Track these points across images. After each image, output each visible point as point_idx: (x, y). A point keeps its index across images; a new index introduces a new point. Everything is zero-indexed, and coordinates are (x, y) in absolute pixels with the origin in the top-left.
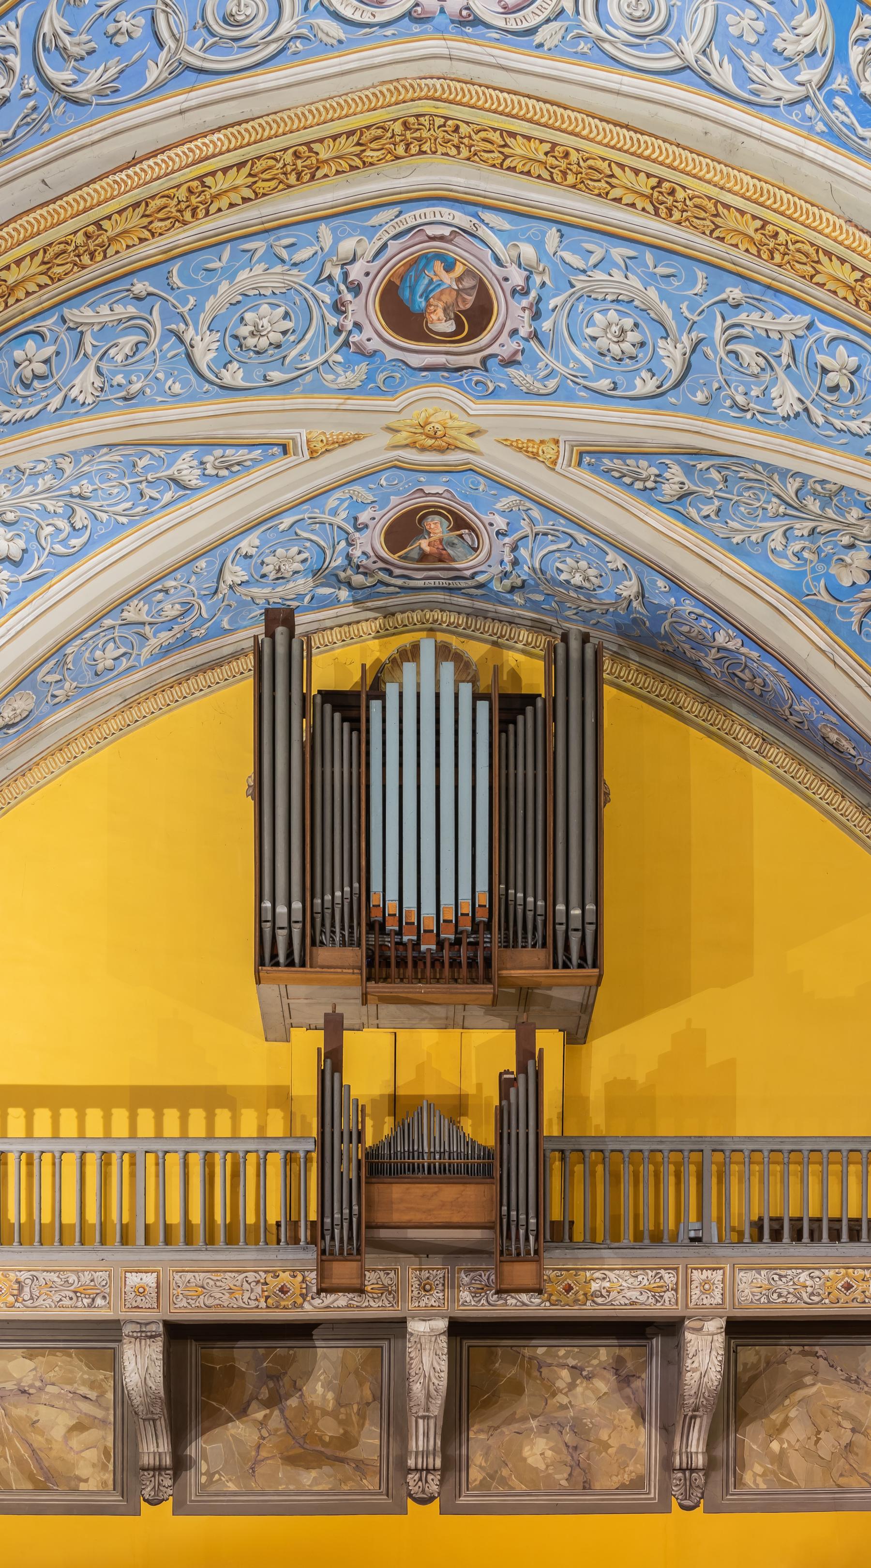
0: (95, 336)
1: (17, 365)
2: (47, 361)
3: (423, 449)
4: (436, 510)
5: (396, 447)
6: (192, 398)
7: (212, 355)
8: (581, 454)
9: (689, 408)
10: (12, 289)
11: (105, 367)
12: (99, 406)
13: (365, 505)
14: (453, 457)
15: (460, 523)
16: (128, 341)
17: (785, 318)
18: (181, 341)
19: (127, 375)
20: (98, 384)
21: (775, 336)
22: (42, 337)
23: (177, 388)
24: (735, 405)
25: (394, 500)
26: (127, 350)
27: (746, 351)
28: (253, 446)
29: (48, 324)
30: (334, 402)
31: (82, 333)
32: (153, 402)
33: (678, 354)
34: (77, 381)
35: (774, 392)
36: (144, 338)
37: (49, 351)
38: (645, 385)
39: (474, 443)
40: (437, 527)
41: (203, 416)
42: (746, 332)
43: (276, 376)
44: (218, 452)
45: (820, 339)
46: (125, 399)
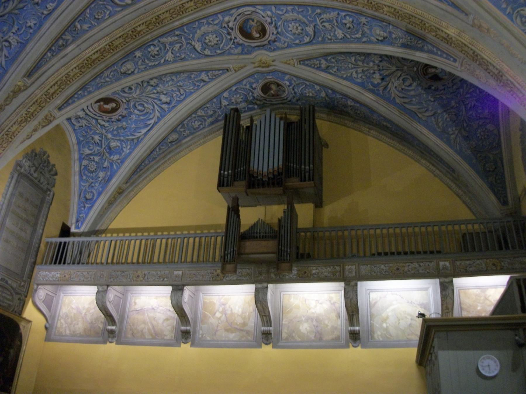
0: (169, 45)
1: (150, 52)
2: (158, 51)
3: (263, 67)
4: (271, 83)
5: (255, 67)
6: (199, 58)
7: (200, 48)
8: (300, 61)
9: (318, 43)
10: (139, 32)
11: (174, 52)
12: (175, 61)
13: (253, 83)
14: (271, 68)
15: (278, 85)
16: (178, 46)
17: (332, 14)
18: (191, 45)
19: (180, 54)
20: (173, 56)
21: (331, 19)
22: (155, 45)
23: (194, 56)
24: (329, 39)
25: (260, 81)
26: (178, 47)
27: (326, 24)
28: (219, 70)
29: (155, 42)
30: (236, 57)
31: (165, 45)
32: (188, 60)
33: (311, 29)
34: (167, 55)
35: (336, 33)
36: (181, 45)
37: (158, 49)
38: (307, 39)
39: (274, 63)
40: (273, 87)
41: (202, 63)
42: (325, 20)
43: (219, 52)
44: (211, 72)
45: (341, 17)
46: (181, 59)
